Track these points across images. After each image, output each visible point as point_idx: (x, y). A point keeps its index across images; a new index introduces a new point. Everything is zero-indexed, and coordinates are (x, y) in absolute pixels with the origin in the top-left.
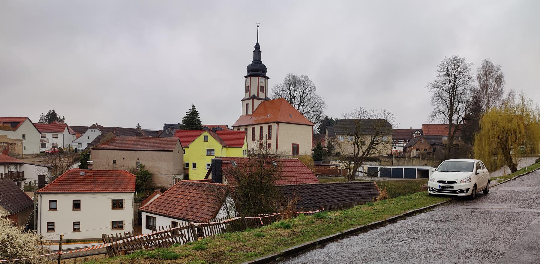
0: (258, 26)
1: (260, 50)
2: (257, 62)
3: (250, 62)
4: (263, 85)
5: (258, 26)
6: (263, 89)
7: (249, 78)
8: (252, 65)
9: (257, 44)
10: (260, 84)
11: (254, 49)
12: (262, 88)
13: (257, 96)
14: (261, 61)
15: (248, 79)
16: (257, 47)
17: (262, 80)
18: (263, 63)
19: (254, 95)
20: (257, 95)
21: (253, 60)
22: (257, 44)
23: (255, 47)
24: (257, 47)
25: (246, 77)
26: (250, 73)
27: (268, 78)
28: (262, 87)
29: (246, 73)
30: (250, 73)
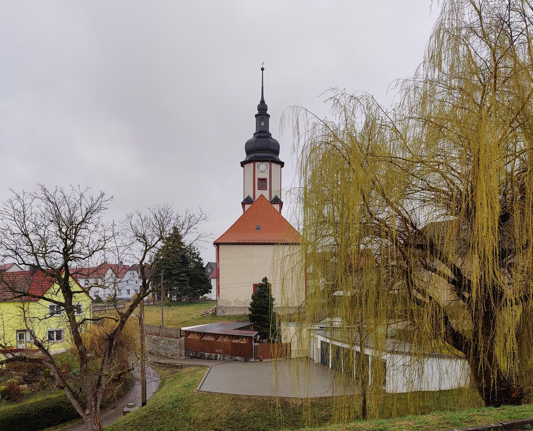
0: (263, 69)
1: (267, 112)
2: (261, 134)
4: (266, 175)
5: (263, 69)
6: (262, 183)
7: (252, 164)
9: (262, 102)
10: (259, 175)
11: (257, 112)
12: (263, 182)
14: (270, 132)
15: (250, 166)
16: (262, 109)
17: (263, 166)
18: (273, 136)
19: (248, 197)
20: (252, 197)
21: (254, 132)
22: (262, 102)
23: (259, 110)
24: (262, 109)
25: (243, 164)
27: (282, 164)
29: (243, 157)
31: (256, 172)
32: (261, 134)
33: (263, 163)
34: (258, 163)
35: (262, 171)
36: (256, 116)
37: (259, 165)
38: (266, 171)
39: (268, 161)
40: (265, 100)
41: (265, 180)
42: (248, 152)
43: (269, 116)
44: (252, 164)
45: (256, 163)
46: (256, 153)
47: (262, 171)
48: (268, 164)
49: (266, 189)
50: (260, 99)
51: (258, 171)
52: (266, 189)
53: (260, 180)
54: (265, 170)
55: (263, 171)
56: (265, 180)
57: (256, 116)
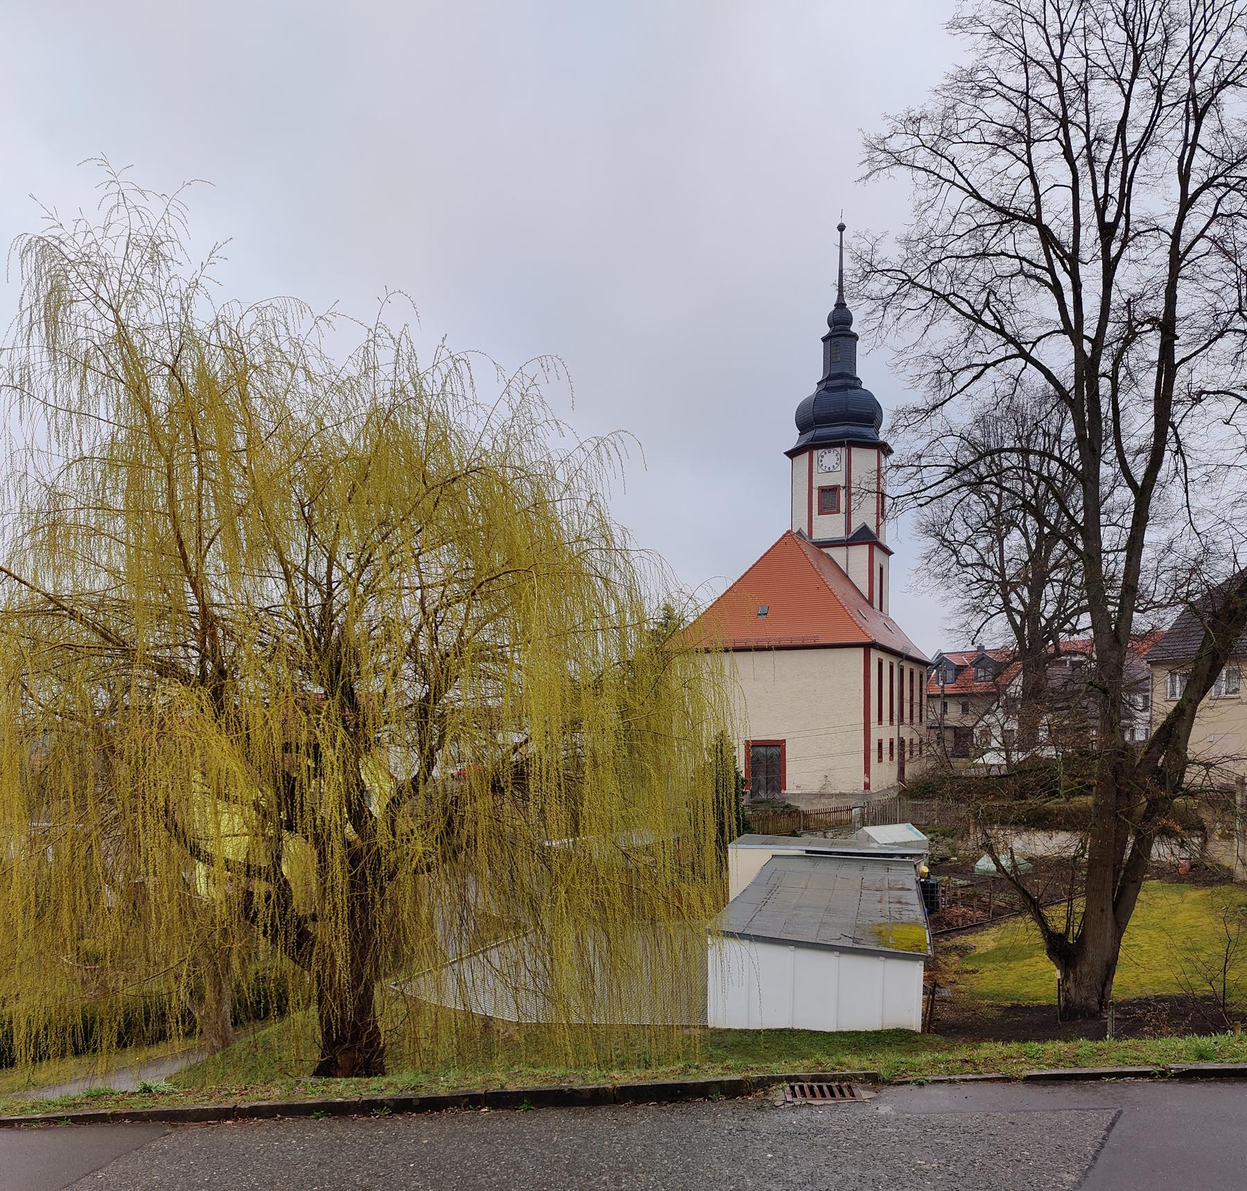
0: (841, 228)
3: (810, 389)
5: (841, 228)
8: (817, 399)
10: (821, 480)
11: (826, 330)
13: (874, 530)
14: (858, 375)
16: (840, 323)
17: (830, 459)
18: (864, 386)
22: (840, 305)
24: (840, 323)
25: (792, 454)
26: (809, 435)
28: (829, 492)
29: (793, 438)
30: (809, 435)
32: (832, 383)
34: (820, 451)
36: (824, 340)
38: (839, 469)
39: (841, 445)
42: (803, 426)
43: (855, 337)
45: (815, 452)
46: (816, 428)
48: (842, 451)
49: (838, 512)
52: (838, 512)
53: (822, 490)
56: (834, 489)
57: (824, 340)
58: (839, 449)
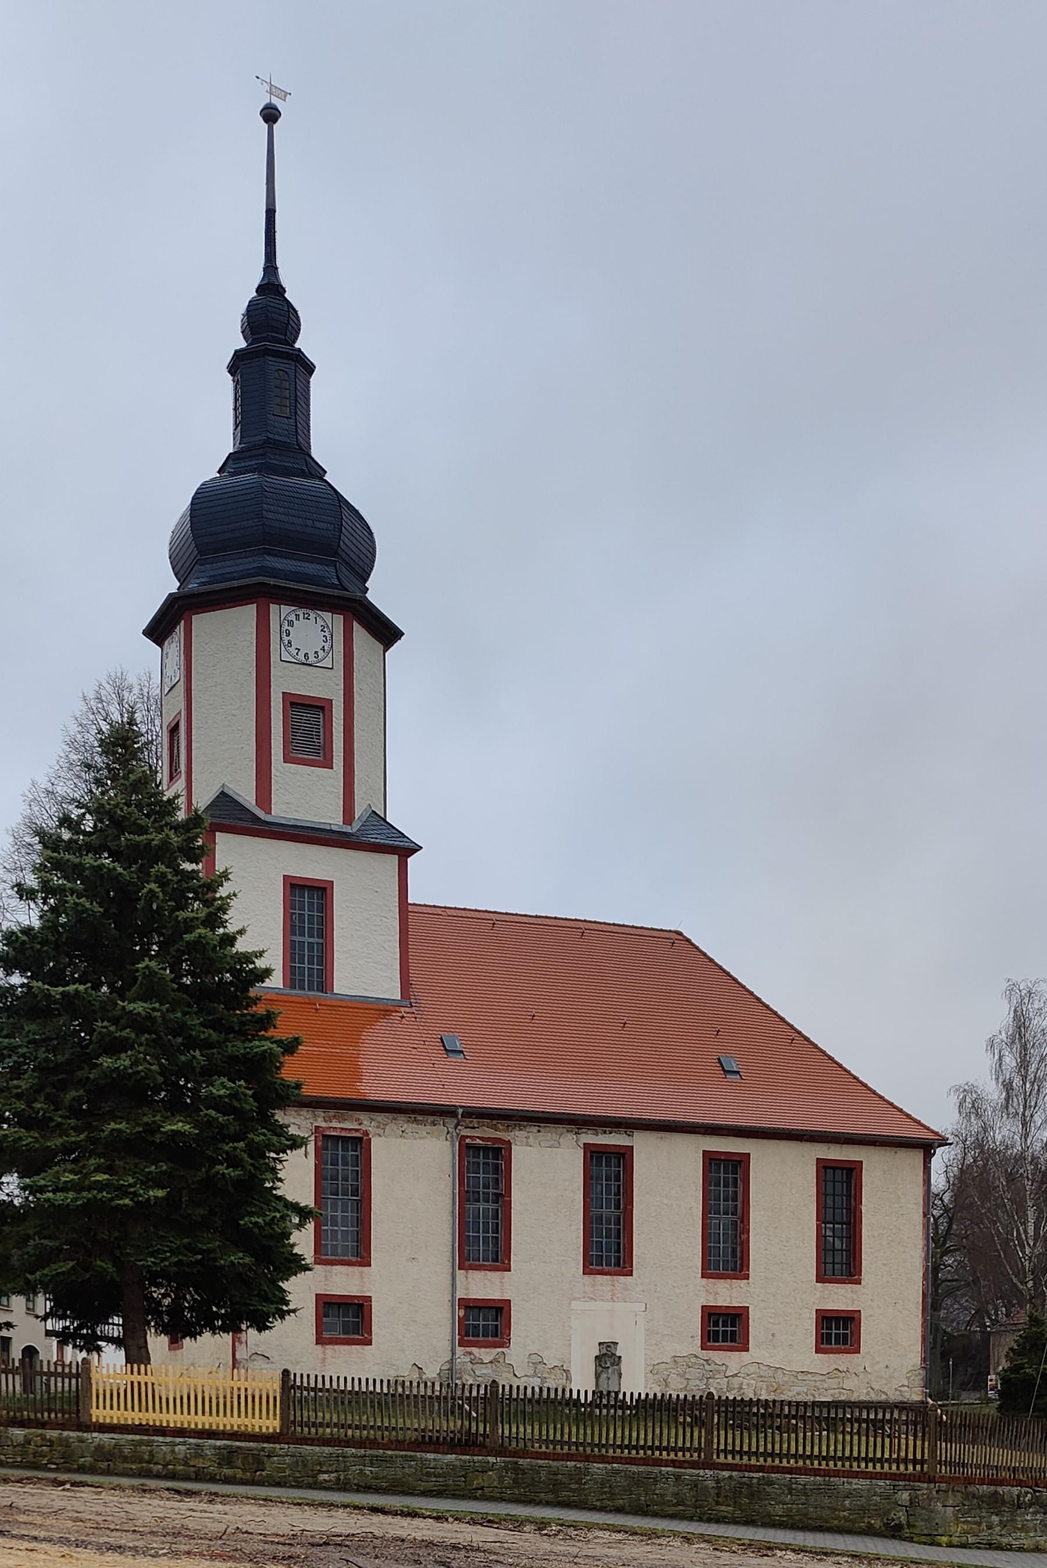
0: (270, 115)
5: (270, 115)
14: (317, 452)
19: (224, 801)
20: (246, 794)
31: (274, 658)
33: (312, 616)
34: (286, 609)
35: (306, 655)
37: (291, 624)
40: (285, 277)
41: (322, 708)
44: (251, 610)
45: (278, 613)
47: (306, 655)
48: (339, 619)
50: (256, 276)
51: (286, 657)
53: (294, 703)
54: (321, 654)
55: (312, 659)
56: (321, 707)
58: (327, 616)
